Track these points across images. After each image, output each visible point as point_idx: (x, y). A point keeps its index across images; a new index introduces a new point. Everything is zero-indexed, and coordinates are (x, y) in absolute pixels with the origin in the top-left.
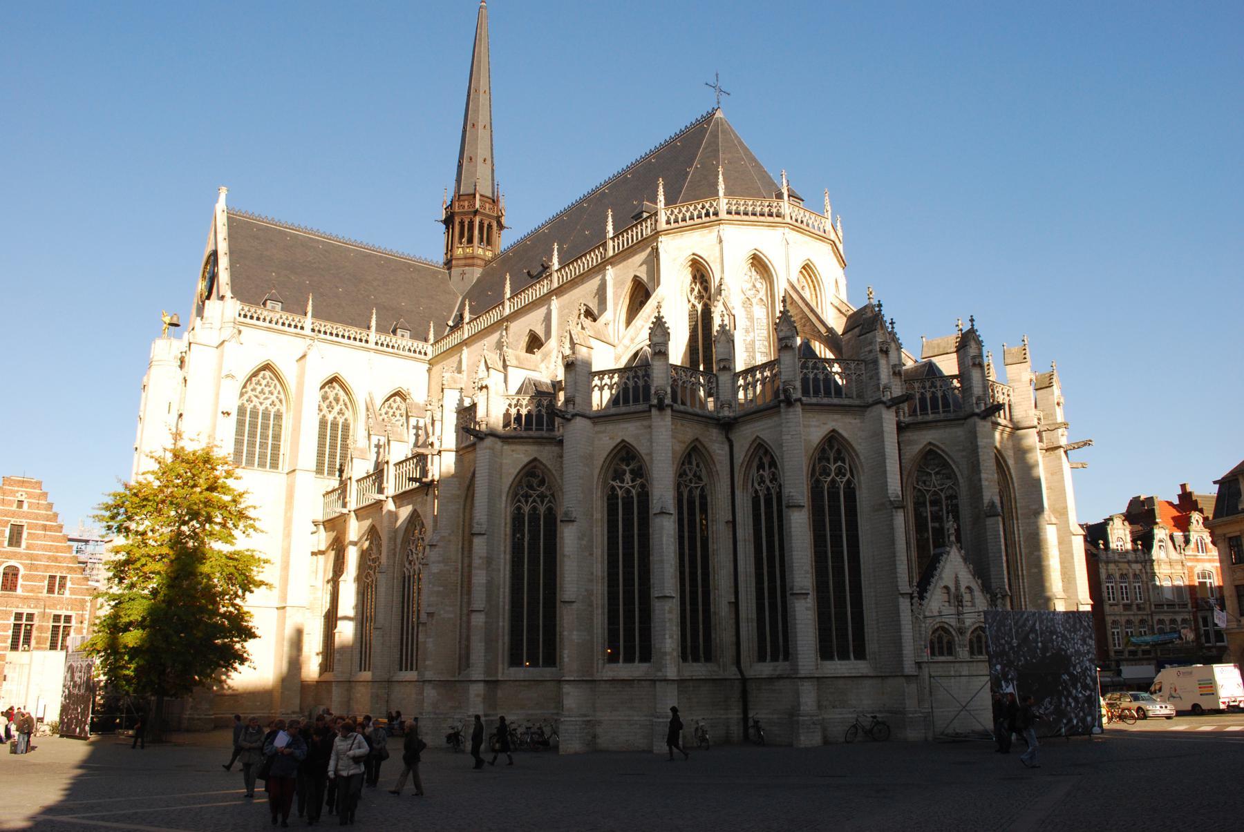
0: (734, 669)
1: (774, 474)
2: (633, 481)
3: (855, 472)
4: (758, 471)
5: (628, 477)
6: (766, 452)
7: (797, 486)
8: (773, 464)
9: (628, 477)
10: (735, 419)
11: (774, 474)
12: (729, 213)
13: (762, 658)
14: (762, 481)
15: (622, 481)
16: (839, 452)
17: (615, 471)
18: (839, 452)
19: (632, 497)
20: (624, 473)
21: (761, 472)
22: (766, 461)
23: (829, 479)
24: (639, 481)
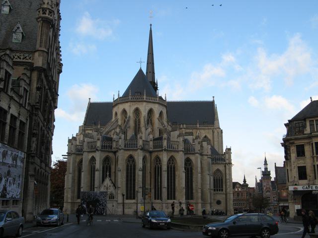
7: (165, 168)
8: (160, 161)
9: (131, 162)
13: (155, 199)
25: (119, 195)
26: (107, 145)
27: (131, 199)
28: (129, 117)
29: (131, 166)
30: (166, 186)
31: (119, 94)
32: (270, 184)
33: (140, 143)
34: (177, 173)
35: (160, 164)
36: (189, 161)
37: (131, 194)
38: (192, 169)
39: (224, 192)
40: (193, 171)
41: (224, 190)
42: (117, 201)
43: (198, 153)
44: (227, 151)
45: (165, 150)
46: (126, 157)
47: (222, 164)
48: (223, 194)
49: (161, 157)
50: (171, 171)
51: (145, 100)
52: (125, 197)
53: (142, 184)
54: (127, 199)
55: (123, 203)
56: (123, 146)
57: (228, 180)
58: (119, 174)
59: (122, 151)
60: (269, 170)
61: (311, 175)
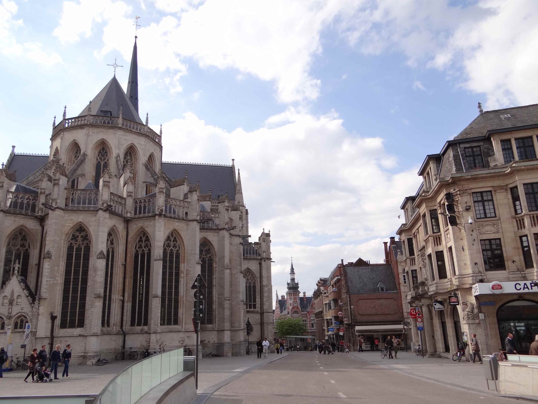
0: (120, 329)
1: (147, 244)
2: (83, 241)
3: (180, 247)
4: (139, 241)
5: (80, 239)
6: (144, 234)
7: (158, 251)
8: (147, 239)
9: (80, 239)
10: (132, 218)
11: (147, 244)
12: (123, 125)
14: (140, 247)
15: (77, 241)
16: (175, 238)
17: (73, 235)
18: (175, 238)
19: (81, 249)
20: (78, 236)
21: (141, 243)
22: (144, 239)
23: (170, 248)
24: (86, 242)
25: (40, 317)
26: (22, 203)
27: (72, 326)
28: (85, 155)
29: (79, 249)
30: (159, 292)
31: (65, 113)
32: (299, 301)
33: (104, 195)
34: (182, 267)
35: (146, 246)
36: (207, 245)
37: (73, 314)
38: (211, 260)
39: (258, 309)
40: (214, 265)
41: (258, 305)
42: (34, 333)
43: (224, 229)
44: (265, 237)
45: (160, 215)
46: (69, 228)
47: (254, 259)
48: (257, 312)
49: (149, 230)
50: (171, 262)
51: (120, 125)
52: (58, 322)
53: (102, 291)
54: (63, 325)
55: (52, 337)
56: (61, 203)
57: (266, 289)
58: (46, 265)
59: (58, 212)
60: (296, 282)
61: (516, 258)
